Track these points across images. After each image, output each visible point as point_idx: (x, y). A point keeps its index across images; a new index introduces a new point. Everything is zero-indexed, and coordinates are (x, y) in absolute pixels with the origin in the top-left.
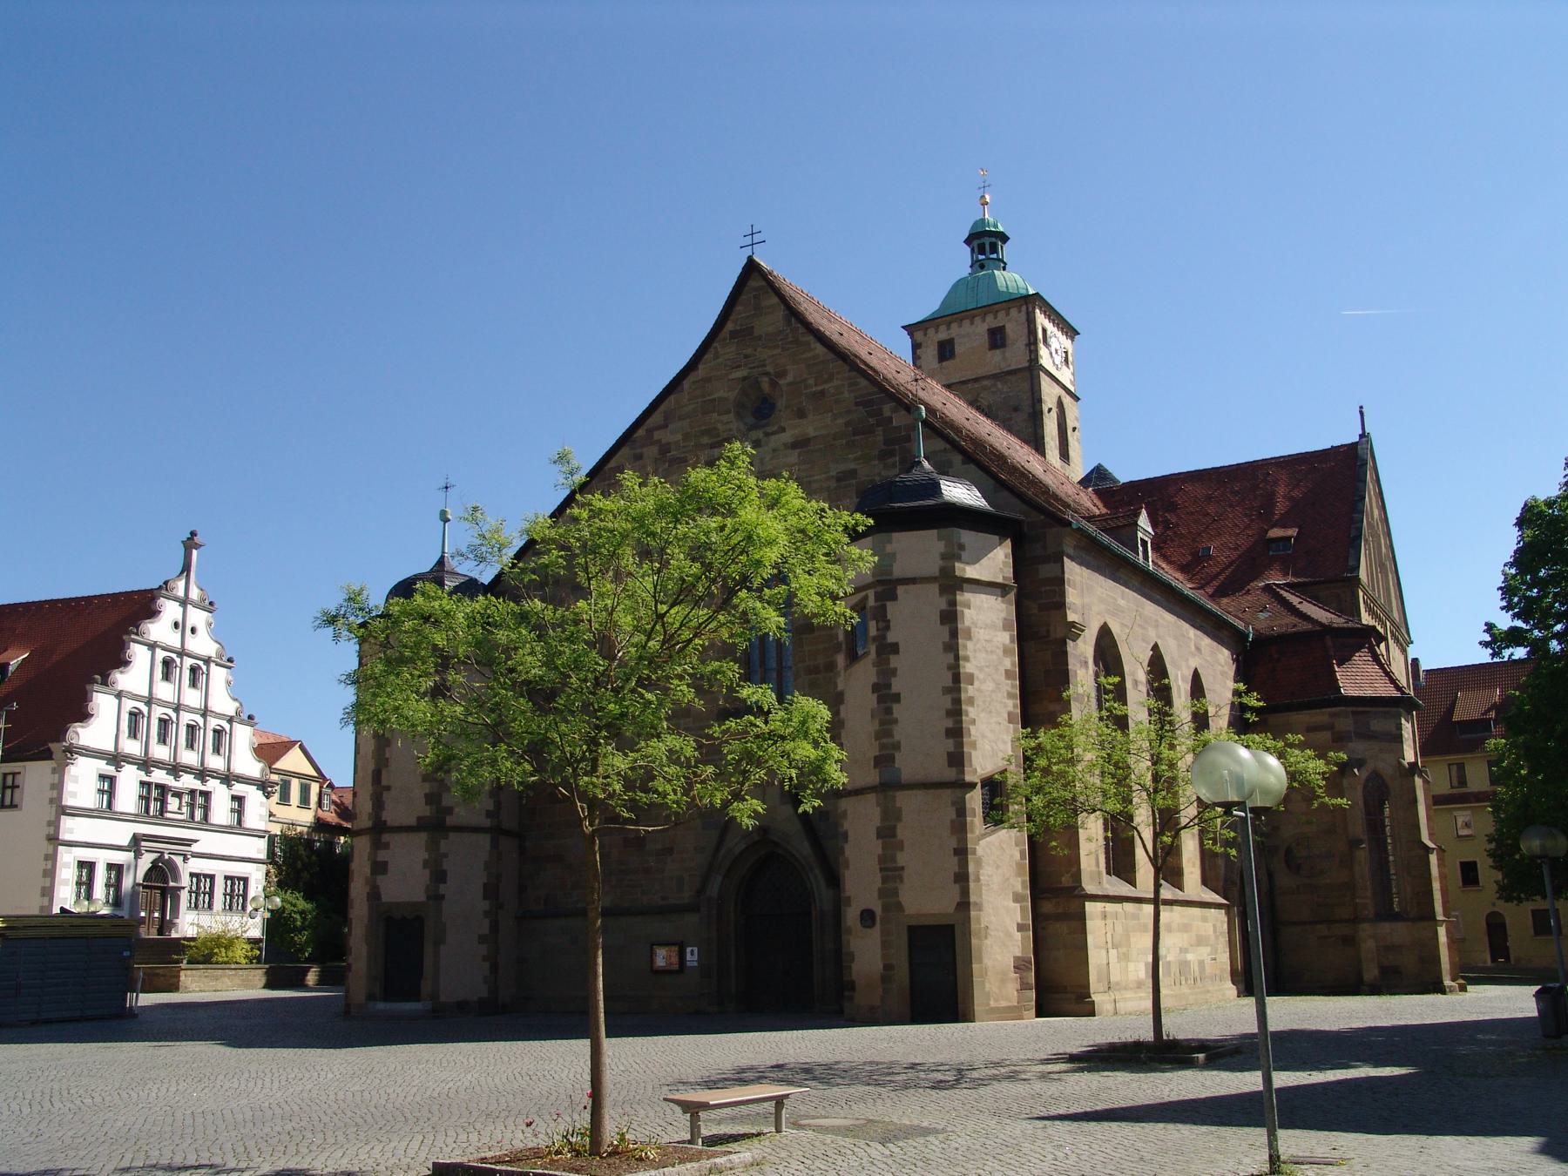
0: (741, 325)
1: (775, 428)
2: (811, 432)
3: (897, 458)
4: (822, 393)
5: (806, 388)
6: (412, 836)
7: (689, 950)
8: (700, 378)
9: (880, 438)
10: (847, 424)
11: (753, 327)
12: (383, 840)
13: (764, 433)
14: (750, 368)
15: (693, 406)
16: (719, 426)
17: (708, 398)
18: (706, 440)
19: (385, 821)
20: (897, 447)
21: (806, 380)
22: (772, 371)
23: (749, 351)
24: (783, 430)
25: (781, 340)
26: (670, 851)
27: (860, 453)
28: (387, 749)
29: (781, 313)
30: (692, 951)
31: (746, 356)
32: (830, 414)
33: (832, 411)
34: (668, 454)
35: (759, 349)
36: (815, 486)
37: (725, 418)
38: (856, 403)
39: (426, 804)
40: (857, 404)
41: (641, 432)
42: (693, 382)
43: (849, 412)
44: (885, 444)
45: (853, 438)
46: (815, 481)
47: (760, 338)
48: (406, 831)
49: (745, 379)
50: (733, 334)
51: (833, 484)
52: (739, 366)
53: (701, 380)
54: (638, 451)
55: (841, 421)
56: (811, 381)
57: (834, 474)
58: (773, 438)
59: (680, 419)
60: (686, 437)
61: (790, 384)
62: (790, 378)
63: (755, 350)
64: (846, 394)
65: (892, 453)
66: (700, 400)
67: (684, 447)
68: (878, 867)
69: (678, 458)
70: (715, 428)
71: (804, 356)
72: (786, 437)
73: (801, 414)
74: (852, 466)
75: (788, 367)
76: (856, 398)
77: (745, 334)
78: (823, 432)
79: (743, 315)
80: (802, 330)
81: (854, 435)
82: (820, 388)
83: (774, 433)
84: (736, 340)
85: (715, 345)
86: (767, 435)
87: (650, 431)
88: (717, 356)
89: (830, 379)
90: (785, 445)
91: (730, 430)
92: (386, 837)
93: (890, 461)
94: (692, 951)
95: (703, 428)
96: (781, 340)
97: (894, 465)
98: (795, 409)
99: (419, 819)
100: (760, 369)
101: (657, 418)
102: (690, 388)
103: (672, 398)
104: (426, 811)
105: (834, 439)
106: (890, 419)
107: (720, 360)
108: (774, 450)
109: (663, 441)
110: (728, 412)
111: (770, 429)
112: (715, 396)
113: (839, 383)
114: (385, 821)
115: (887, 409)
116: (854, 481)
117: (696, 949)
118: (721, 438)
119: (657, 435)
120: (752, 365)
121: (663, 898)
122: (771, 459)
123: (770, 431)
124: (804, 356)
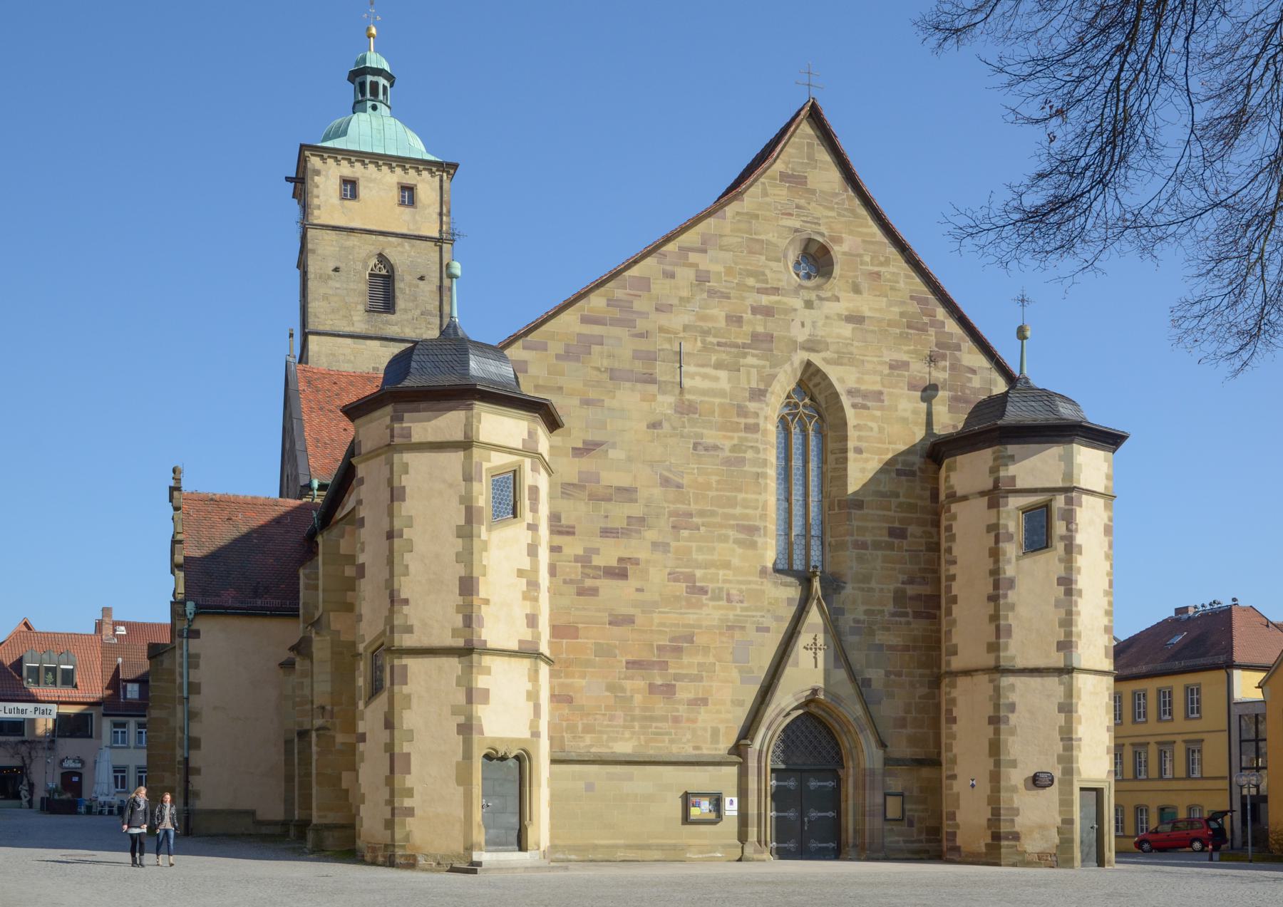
0: (793, 170)
1: (829, 294)
2: (867, 313)
3: (948, 364)
4: (878, 274)
5: (862, 263)
6: (515, 662)
7: (727, 800)
8: (745, 211)
9: (933, 339)
10: (902, 314)
11: (806, 177)
12: (483, 664)
13: (817, 296)
14: (803, 221)
15: (740, 240)
16: (767, 272)
17: (754, 236)
18: (751, 282)
19: (485, 641)
20: (948, 352)
21: (860, 256)
22: (826, 234)
23: (802, 202)
24: (838, 299)
25: (837, 203)
26: (704, 701)
27: (912, 347)
28: (484, 554)
29: (835, 175)
30: (732, 801)
31: (798, 207)
32: (885, 299)
33: (887, 296)
34: (707, 284)
35: (813, 204)
36: (868, 366)
37: (773, 264)
38: (911, 296)
39: (528, 627)
40: (912, 298)
41: (671, 247)
42: (738, 213)
43: (903, 303)
44: (936, 345)
45: (906, 330)
46: (868, 362)
47: (813, 192)
48: (510, 656)
49: (796, 230)
50: (784, 177)
51: (887, 371)
52: (791, 215)
53: (747, 214)
54: (669, 268)
55: (896, 309)
56: (867, 259)
57: (888, 360)
58: (827, 303)
59: (722, 248)
60: (729, 271)
61: (845, 254)
62: (845, 247)
63: (809, 203)
64: (902, 285)
65: (944, 357)
66: (745, 236)
67: (725, 281)
68: (1059, 738)
69: (719, 291)
70: (764, 274)
71: (860, 230)
72: (843, 307)
73: (856, 290)
74: (905, 358)
75: (843, 235)
76: (911, 291)
77: (795, 180)
78: (877, 315)
79: (796, 160)
80: (857, 202)
81: (909, 327)
82: (876, 269)
83: (827, 299)
84: (787, 185)
85: (762, 180)
86: (820, 299)
87: (684, 250)
88: (765, 194)
89: (887, 262)
90: (839, 316)
91: (779, 280)
92: (487, 660)
93: (942, 364)
94: (732, 801)
95: (749, 267)
96: (837, 203)
97: (944, 369)
98: (850, 281)
99: (520, 642)
100: (813, 226)
101: (689, 238)
102: (734, 218)
103: (711, 221)
104: (527, 634)
105: (889, 325)
106: (943, 323)
107: (768, 199)
108: (827, 317)
109: (701, 267)
110: (778, 260)
111: (823, 294)
112: (760, 237)
113: (895, 270)
114: (485, 641)
115: (941, 313)
116: (906, 373)
117: (735, 800)
118: (769, 286)
119: (693, 257)
120: (805, 219)
121: (697, 748)
122: (824, 326)
123: (823, 296)
124: (860, 230)
